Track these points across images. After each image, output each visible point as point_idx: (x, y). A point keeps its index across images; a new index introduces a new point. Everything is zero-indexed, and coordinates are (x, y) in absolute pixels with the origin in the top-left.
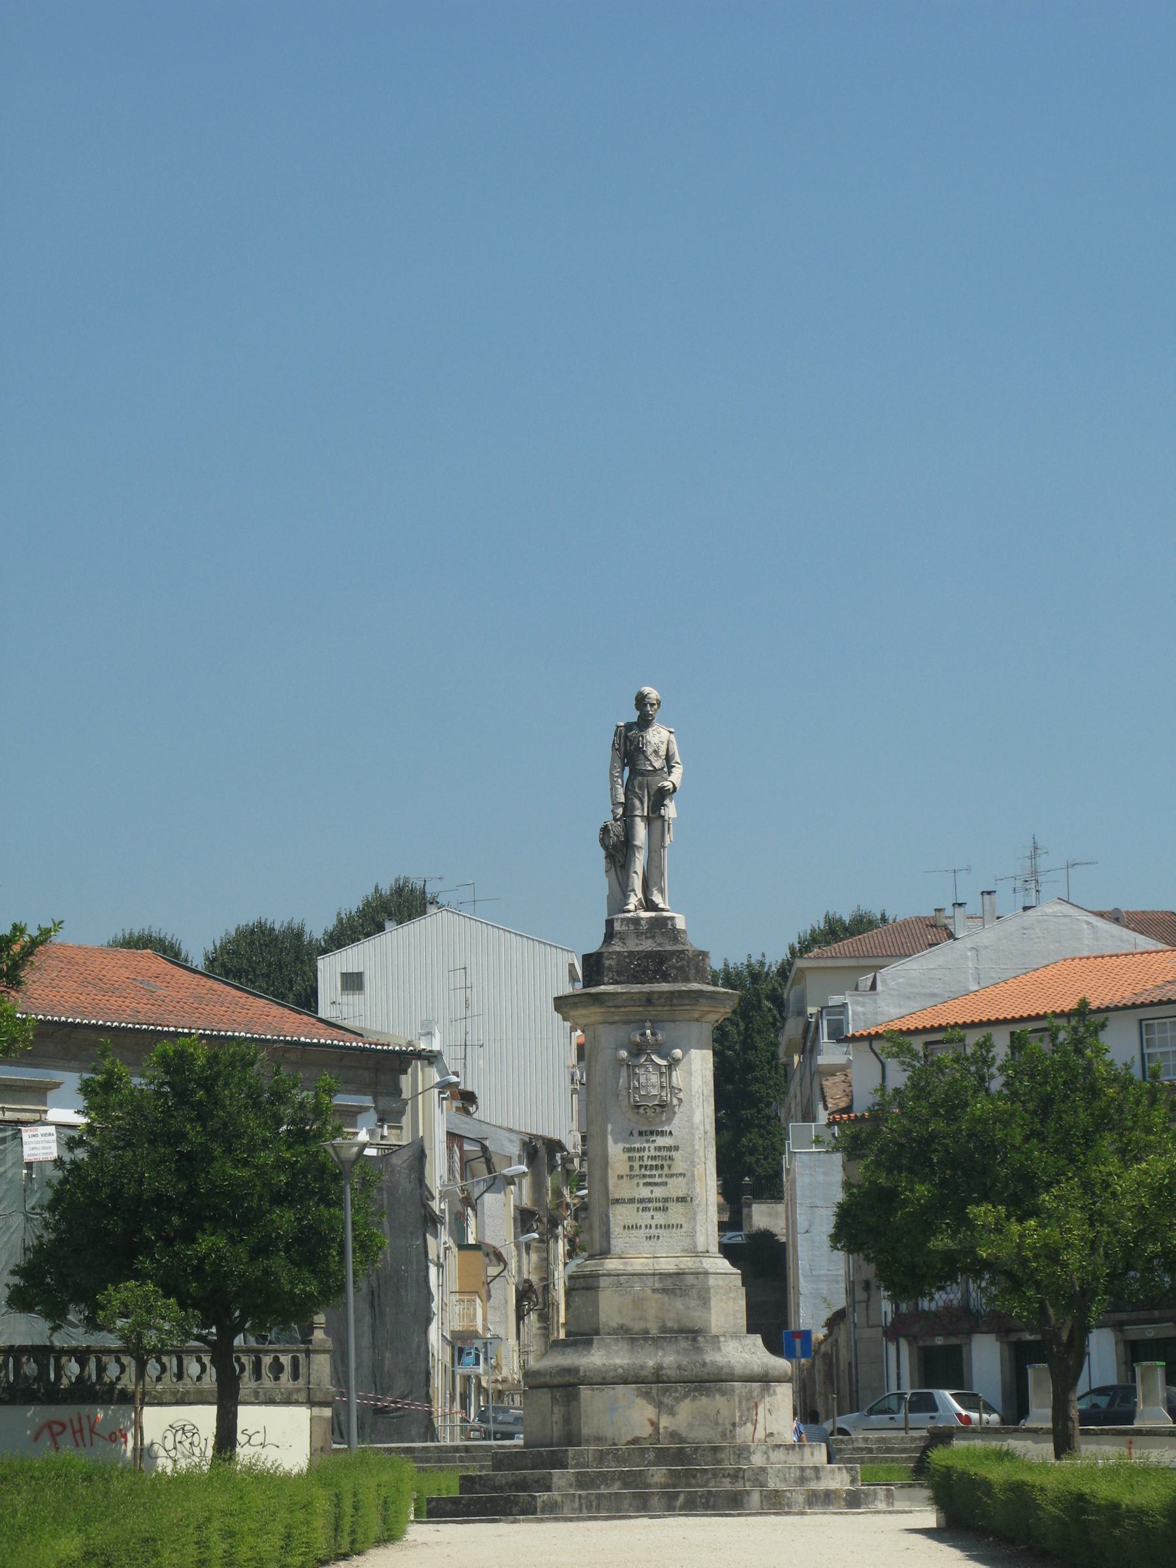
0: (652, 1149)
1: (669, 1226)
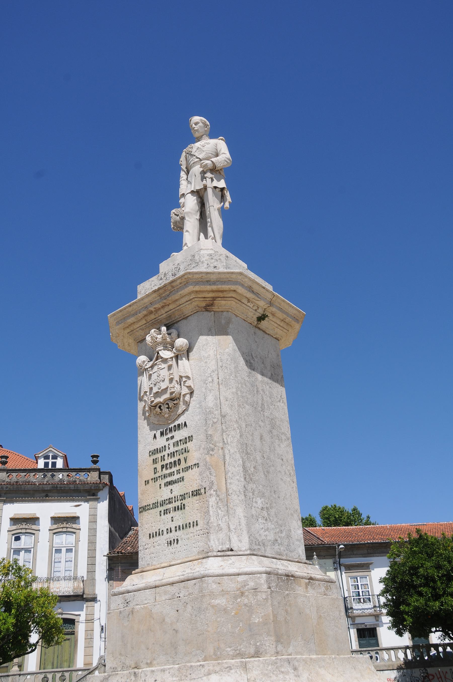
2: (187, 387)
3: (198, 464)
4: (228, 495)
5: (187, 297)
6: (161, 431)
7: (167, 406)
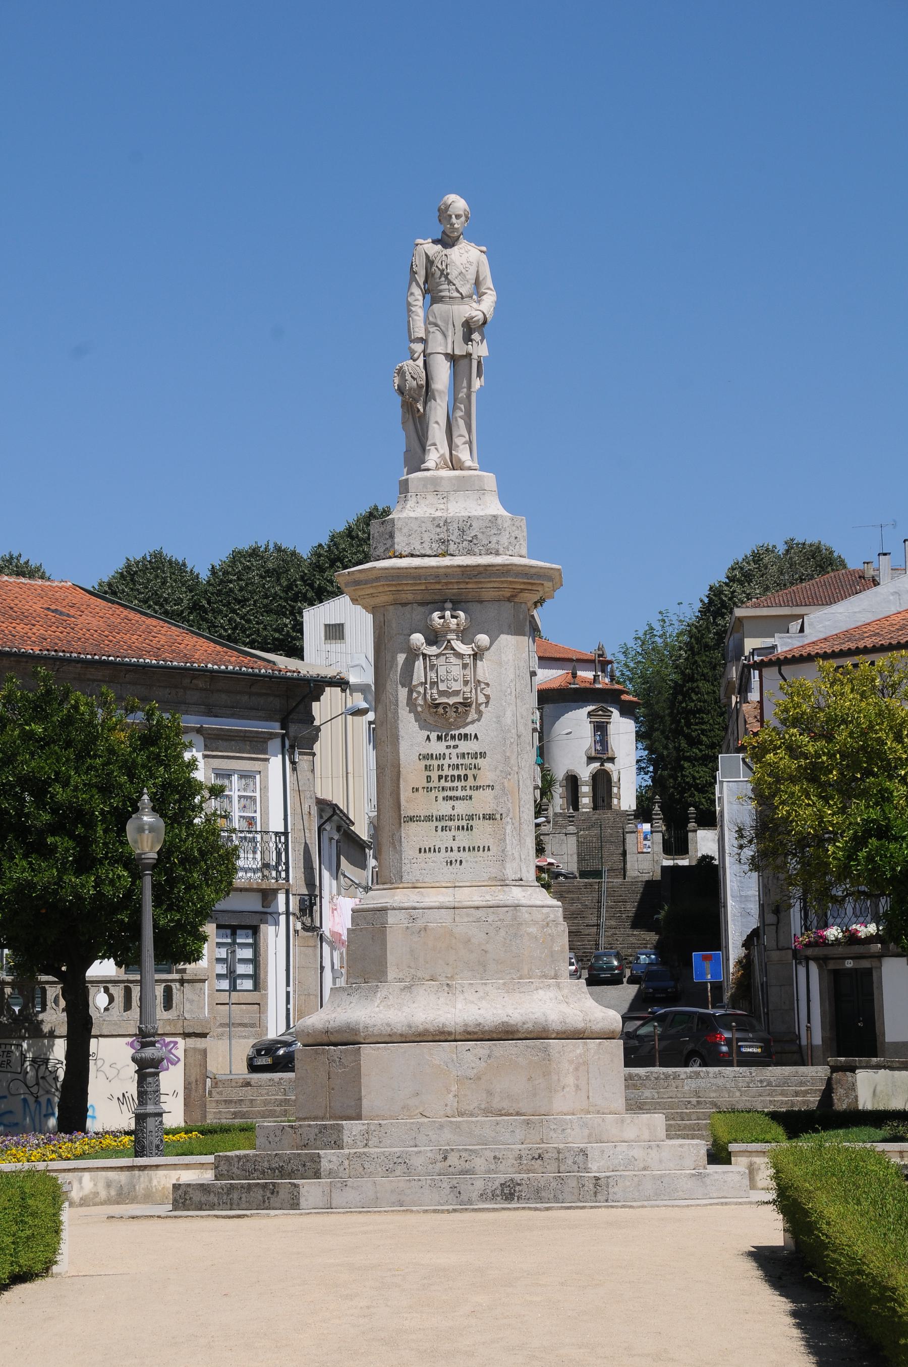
0: (454, 756)
1: (474, 848)
2: (485, 695)
4: (520, 824)
6: (438, 735)
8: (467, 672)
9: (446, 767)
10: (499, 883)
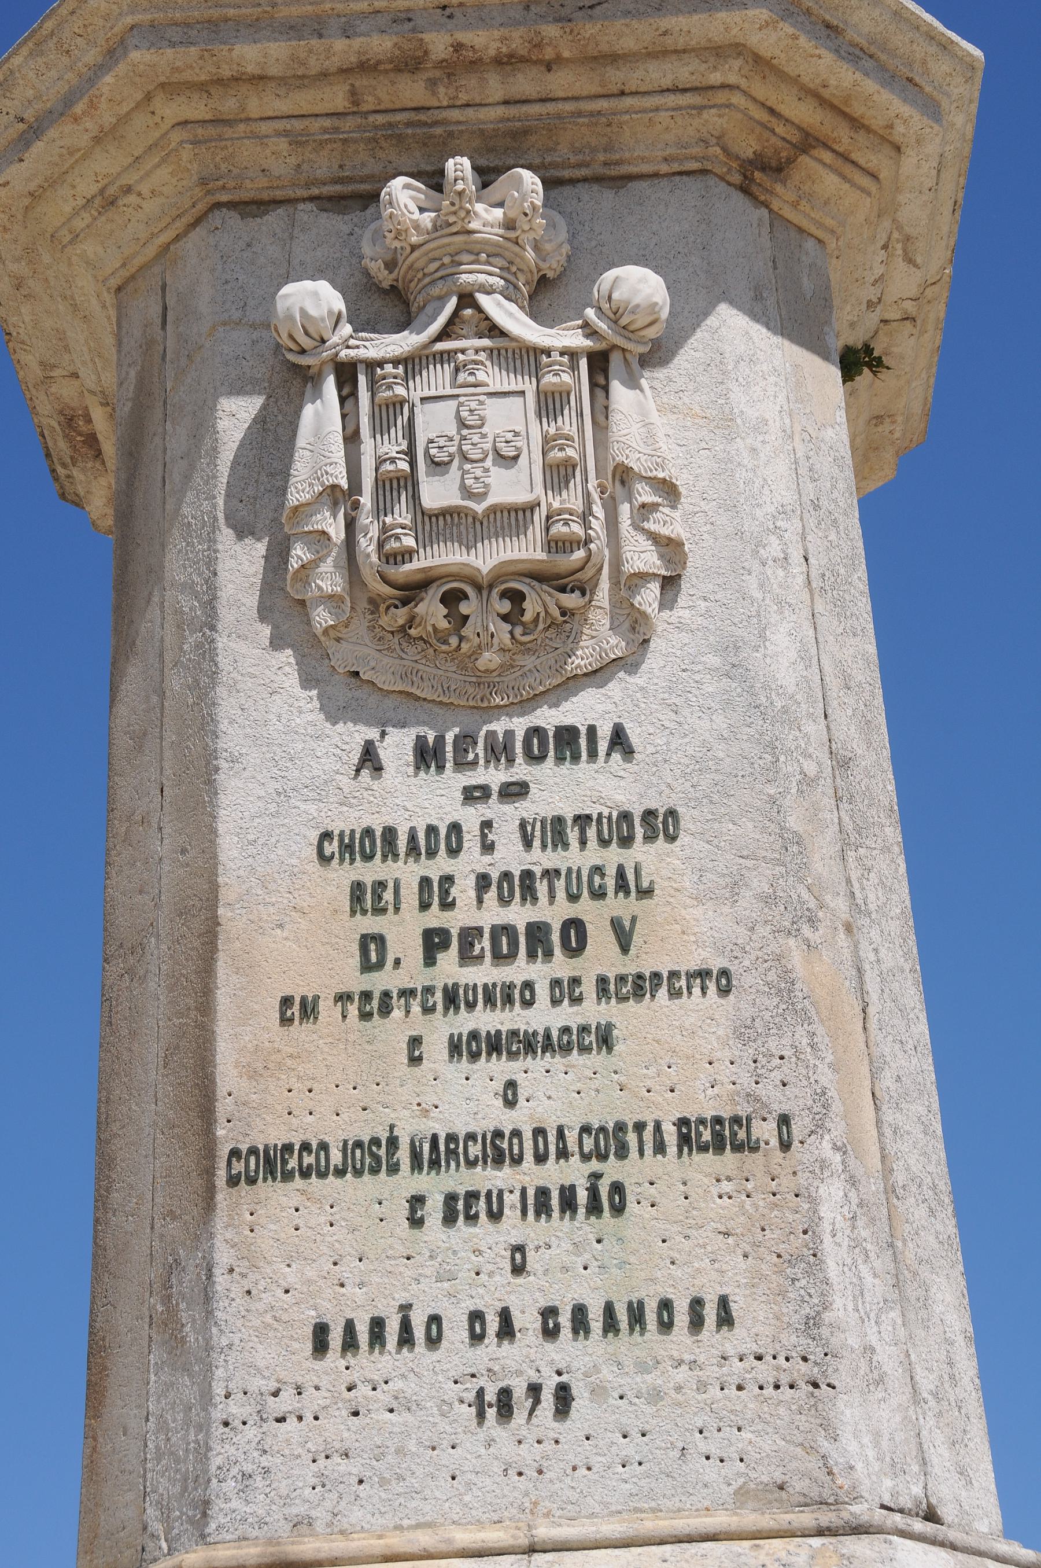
2: (655, 538)
3: (724, 973)
4: (890, 1190)
5: (695, 64)
6: (420, 743)
7: (505, 606)
8: (567, 424)
9: (464, 891)
10: (806, 1519)
